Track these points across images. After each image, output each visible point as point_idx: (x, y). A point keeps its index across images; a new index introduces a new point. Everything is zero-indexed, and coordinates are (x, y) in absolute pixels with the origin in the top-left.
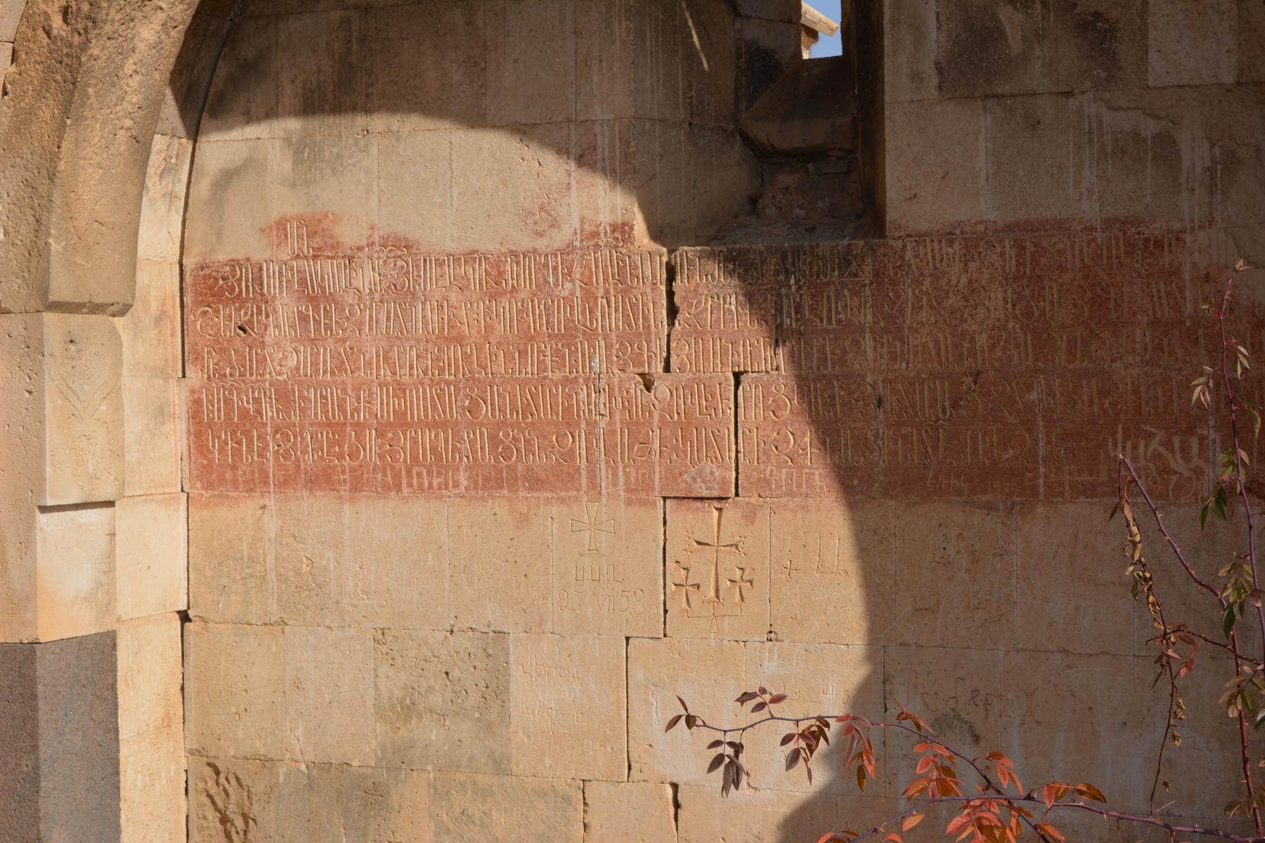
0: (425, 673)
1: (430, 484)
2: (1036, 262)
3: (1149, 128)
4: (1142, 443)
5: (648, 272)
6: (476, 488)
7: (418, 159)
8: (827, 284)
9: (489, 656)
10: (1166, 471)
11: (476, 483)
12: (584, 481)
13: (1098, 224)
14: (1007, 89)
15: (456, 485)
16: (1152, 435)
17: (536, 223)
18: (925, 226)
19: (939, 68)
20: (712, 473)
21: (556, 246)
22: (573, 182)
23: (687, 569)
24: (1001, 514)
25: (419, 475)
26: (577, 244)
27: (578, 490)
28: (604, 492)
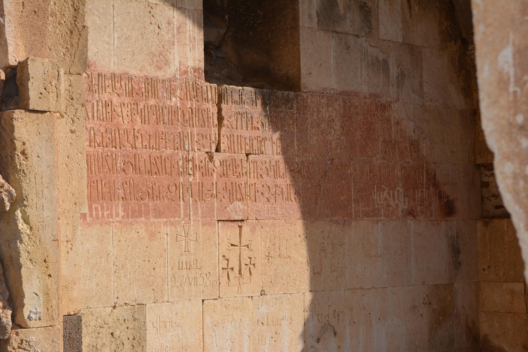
0: (100, 335)
1: (103, 214)
2: (350, 110)
3: (381, 57)
4: (382, 193)
5: (210, 97)
6: (128, 217)
7: (95, 12)
8: (281, 112)
9: (135, 319)
10: (389, 206)
11: (128, 214)
12: (182, 212)
13: (367, 96)
14: (339, 29)
15: (117, 215)
16: (384, 190)
17: (157, 61)
18: (314, 88)
19: (318, 15)
20: (239, 207)
21: (168, 76)
22: (176, 41)
23: (228, 260)
24: (341, 226)
25: (96, 209)
26: (178, 76)
27: (179, 217)
28: (192, 218)
